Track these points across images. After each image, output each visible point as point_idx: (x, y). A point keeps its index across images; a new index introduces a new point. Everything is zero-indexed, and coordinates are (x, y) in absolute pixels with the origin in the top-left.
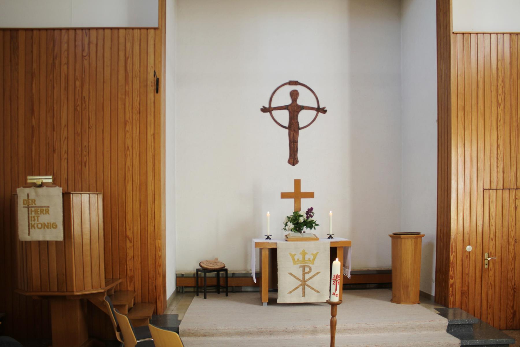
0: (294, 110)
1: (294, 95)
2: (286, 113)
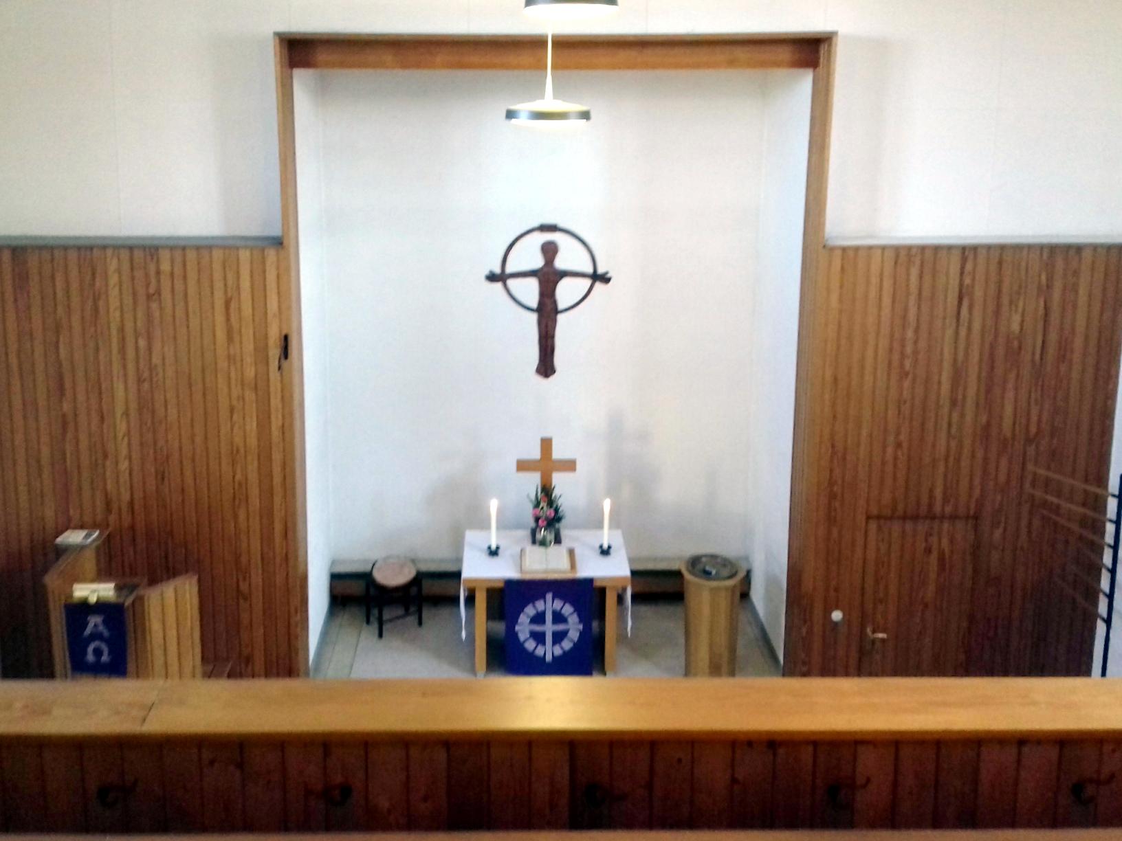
0: (549, 278)
1: (550, 251)
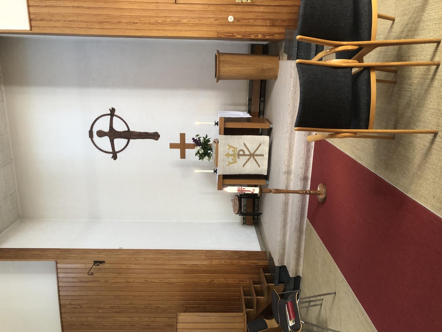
0: (113, 134)
1: (101, 134)
2: (116, 141)
